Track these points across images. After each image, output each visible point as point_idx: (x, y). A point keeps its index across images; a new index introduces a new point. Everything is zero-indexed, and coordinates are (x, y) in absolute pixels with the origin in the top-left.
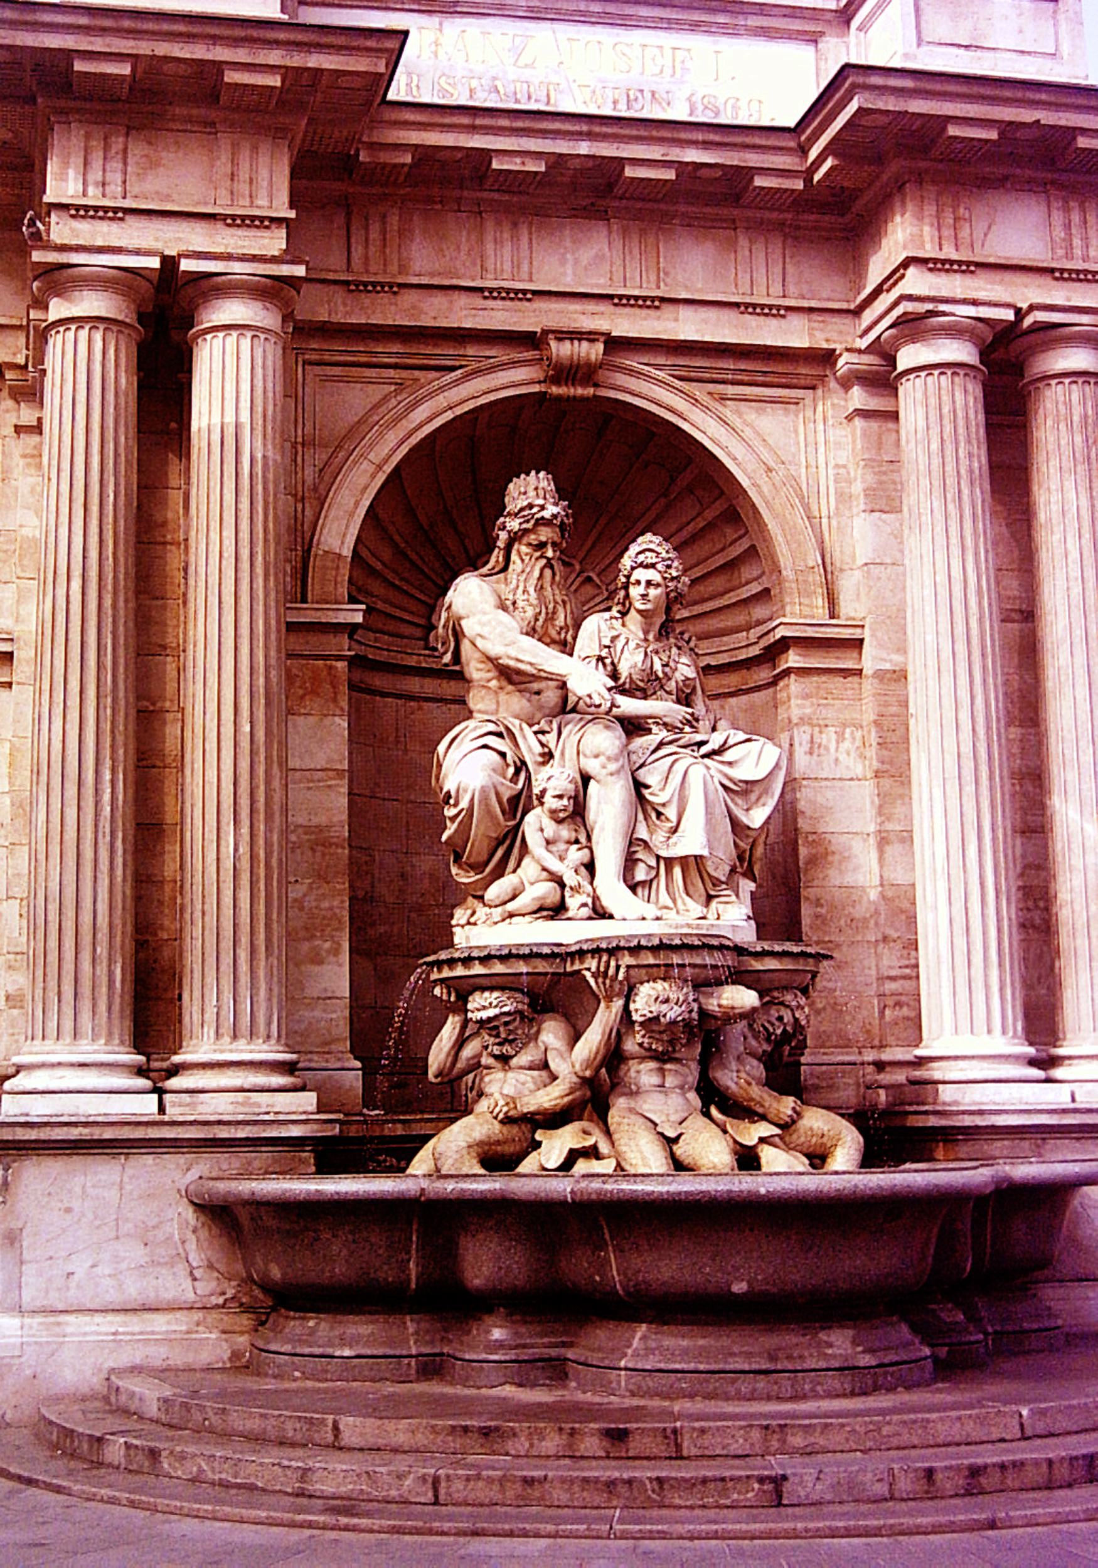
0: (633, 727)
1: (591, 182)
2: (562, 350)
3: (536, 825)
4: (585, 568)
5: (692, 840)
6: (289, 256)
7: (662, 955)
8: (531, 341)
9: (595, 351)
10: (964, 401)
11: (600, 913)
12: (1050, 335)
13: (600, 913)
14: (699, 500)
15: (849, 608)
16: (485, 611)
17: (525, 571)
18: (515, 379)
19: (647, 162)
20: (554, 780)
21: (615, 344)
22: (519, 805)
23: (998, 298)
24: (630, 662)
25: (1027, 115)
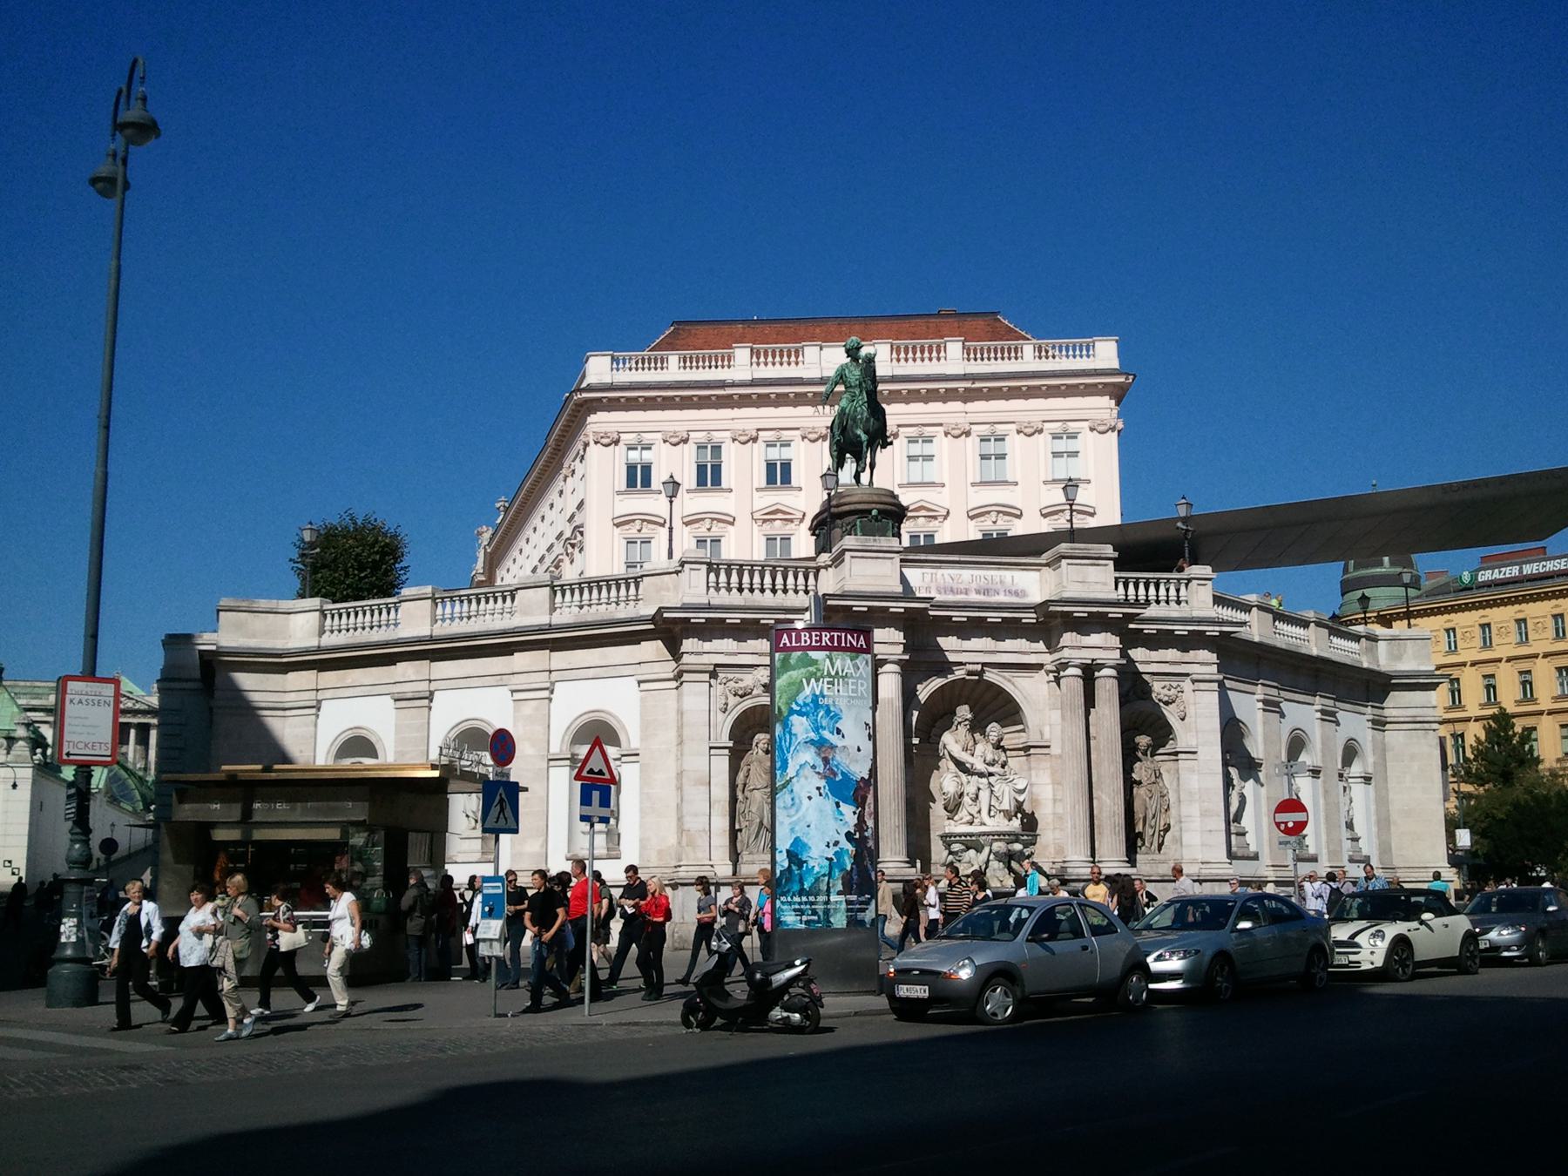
3: (966, 799)
4: (978, 726)
5: (1005, 806)
6: (904, 652)
7: (1000, 835)
10: (1079, 685)
11: (983, 824)
12: (1101, 666)
13: (983, 824)
14: (1004, 710)
15: (1047, 736)
16: (953, 741)
17: (963, 730)
19: (994, 617)
20: (970, 789)
21: (984, 664)
22: (961, 795)
23: (1087, 656)
24: (989, 758)
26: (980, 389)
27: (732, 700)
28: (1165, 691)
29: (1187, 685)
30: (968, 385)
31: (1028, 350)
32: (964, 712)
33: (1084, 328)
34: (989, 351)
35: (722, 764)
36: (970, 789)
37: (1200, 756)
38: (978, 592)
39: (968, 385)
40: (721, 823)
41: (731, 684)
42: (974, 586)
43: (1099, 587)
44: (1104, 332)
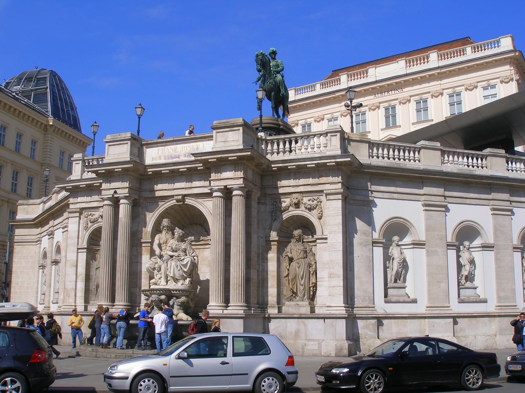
0: (172, 257)
1: (173, 174)
2: (176, 197)
8: (173, 196)
9: (180, 197)
18: (173, 202)
21: (184, 196)
25: (220, 156)
26: (445, 72)
27: (90, 224)
28: (311, 202)
29: (323, 198)
30: (439, 71)
31: (469, 49)
32: (165, 222)
33: (494, 35)
34: (454, 53)
35: (83, 257)
36: (156, 266)
37: (328, 241)
38: (185, 156)
39: (439, 71)
40: (81, 285)
41: (90, 216)
42: (183, 152)
43: (233, 144)
44: (504, 34)
